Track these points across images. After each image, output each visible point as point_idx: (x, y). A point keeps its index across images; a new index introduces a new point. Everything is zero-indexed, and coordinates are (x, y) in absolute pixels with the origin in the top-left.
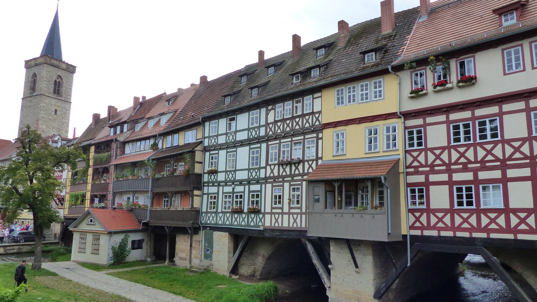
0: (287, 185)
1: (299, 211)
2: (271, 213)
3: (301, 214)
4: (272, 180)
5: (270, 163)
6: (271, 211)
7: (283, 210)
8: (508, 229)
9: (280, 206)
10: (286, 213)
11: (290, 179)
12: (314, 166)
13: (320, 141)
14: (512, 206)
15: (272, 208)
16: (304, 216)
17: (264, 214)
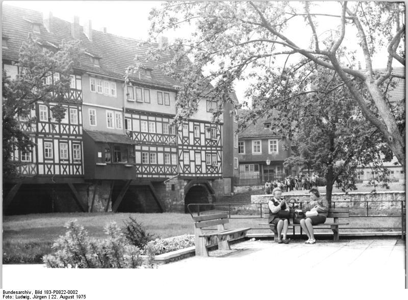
0: (56, 142)
1: (67, 162)
2: (44, 164)
3: (69, 164)
4: (43, 136)
5: (41, 120)
6: (44, 161)
7: (54, 161)
8: (157, 174)
9: (52, 157)
10: (57, 164)
11: (58, 136)
12: (77, 129)
13: (80, 112)
14: (159, 163)
15: (44, 159)
16: (71, 167)
17: (37, 164)
